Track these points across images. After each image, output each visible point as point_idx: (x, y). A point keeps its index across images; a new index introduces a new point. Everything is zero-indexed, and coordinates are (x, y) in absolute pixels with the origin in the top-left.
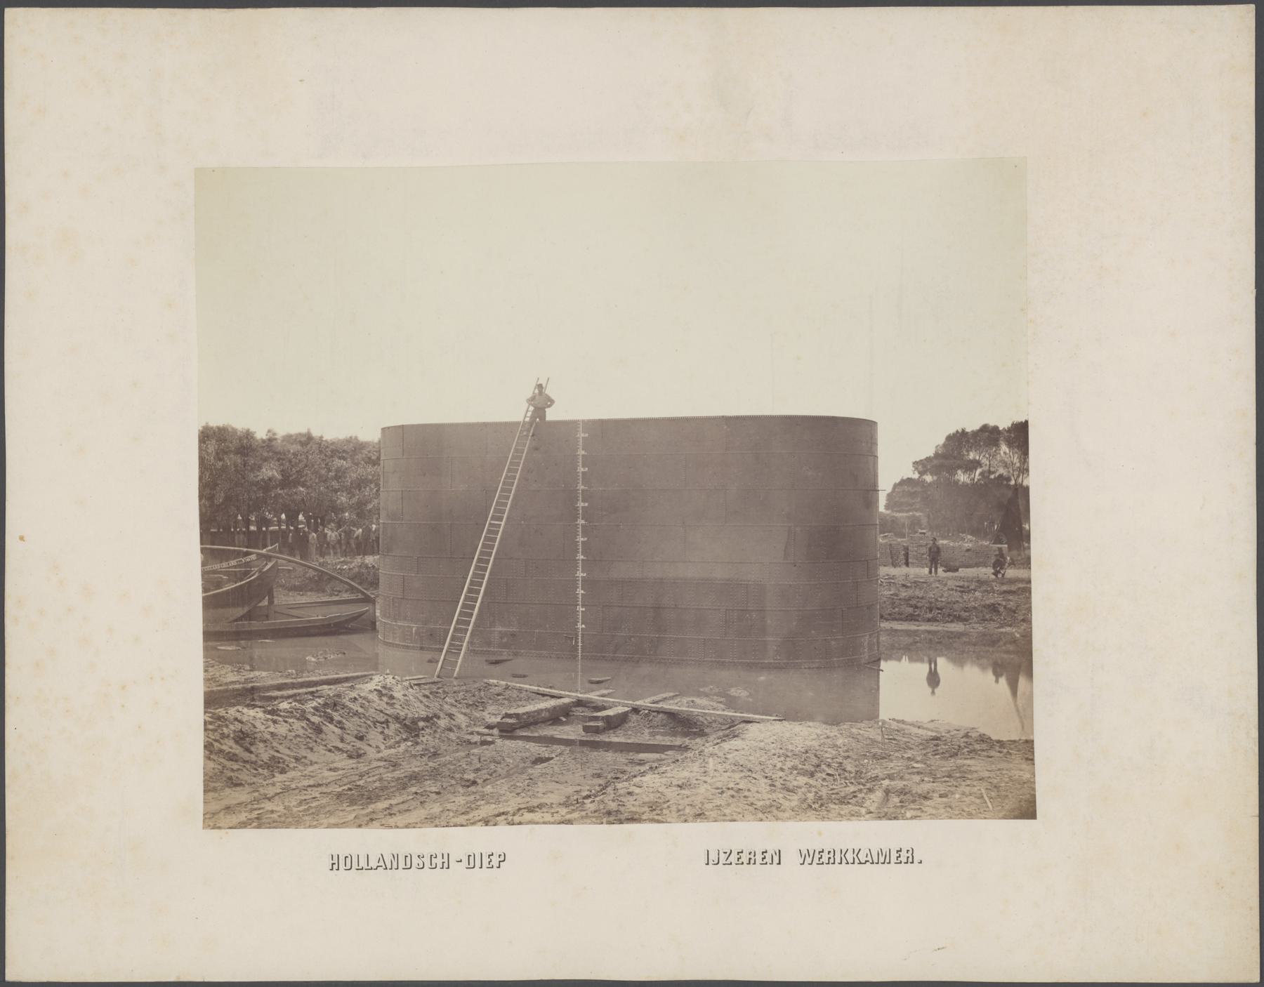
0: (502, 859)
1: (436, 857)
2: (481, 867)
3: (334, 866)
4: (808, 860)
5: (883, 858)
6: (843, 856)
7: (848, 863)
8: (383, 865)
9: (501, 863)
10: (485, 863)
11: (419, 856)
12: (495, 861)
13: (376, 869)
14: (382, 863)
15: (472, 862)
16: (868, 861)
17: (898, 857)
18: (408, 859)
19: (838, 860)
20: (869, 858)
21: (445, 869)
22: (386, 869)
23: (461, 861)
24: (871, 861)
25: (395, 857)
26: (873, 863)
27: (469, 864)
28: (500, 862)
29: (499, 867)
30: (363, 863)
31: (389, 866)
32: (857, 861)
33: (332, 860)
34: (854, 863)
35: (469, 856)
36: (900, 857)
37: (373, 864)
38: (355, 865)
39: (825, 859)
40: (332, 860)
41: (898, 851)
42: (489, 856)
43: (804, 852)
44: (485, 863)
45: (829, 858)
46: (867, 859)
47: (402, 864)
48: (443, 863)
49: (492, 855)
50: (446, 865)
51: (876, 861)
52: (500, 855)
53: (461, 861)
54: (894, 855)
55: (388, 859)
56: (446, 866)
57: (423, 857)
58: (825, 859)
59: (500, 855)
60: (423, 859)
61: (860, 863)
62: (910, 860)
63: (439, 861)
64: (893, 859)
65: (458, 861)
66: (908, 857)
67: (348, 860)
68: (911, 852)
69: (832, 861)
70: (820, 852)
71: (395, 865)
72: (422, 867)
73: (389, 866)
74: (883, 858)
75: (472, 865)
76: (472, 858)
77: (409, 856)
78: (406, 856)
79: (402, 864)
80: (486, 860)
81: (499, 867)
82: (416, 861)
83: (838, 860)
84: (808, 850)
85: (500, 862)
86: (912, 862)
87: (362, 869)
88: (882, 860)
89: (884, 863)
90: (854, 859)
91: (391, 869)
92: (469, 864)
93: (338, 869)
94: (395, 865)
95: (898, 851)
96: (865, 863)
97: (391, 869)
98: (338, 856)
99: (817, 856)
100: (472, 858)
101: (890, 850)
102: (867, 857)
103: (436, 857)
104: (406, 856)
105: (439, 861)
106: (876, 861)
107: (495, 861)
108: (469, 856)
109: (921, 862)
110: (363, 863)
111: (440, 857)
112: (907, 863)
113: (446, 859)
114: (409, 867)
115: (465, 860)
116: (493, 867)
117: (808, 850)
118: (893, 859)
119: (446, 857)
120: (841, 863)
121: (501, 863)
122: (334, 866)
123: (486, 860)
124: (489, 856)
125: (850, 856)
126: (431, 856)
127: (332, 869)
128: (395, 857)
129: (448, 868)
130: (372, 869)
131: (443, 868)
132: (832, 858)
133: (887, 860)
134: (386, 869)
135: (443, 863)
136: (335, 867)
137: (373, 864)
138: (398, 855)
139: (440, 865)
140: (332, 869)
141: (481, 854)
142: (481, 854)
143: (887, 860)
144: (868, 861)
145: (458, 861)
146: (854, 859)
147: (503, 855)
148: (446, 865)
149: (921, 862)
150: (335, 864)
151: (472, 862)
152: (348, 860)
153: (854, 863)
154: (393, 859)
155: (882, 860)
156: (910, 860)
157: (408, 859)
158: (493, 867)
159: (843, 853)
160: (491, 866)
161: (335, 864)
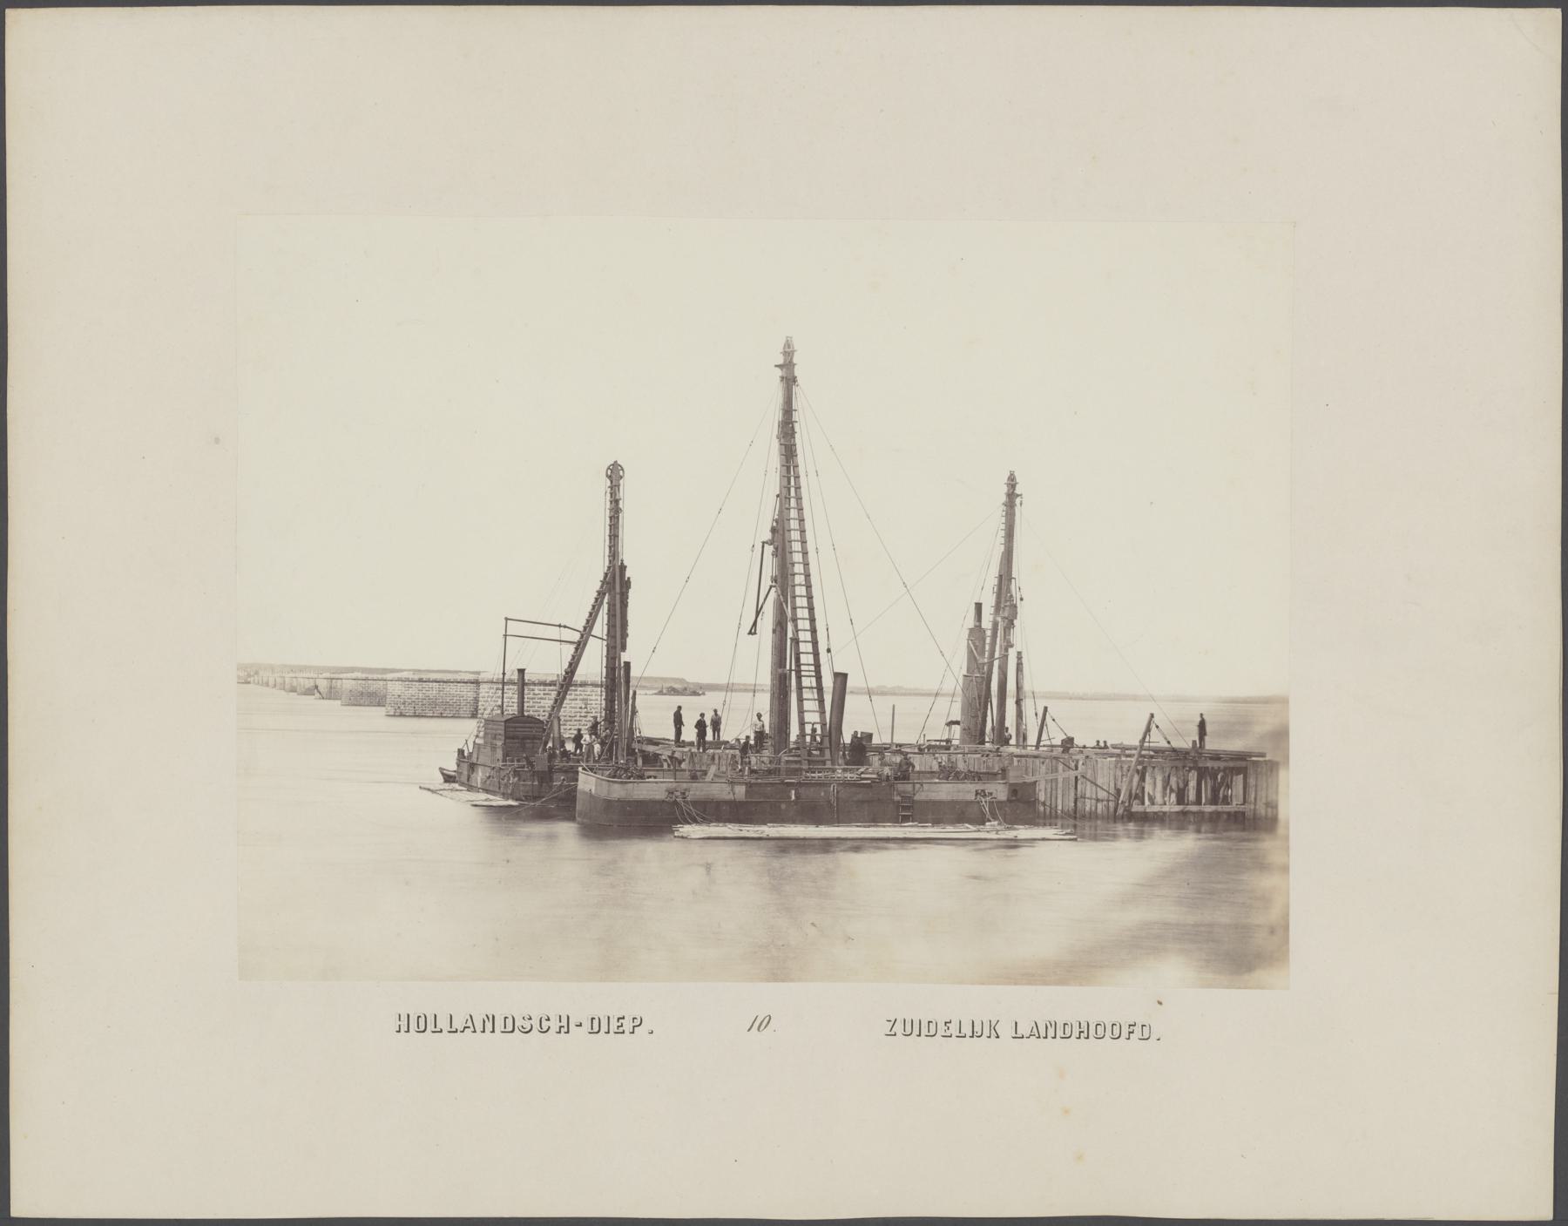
2: (608, 1032)
8: (470, 1025)
12: (628, 1025)
13: (463, 1032)
14: (470, 1024)
15: (596, 1026)
22: (475, 1032)
23: (581, 1025)
27: (592, 1029)
28: (634, 1027)
29: (633, 1033)
30: (443, 1023)
35: (593, 1019)
37: (458, 1024)
38: (430, 1027)
44: (613, 1027)
49: (623, 1018)
53: (581, 1025)
57: (530, 1019)
65: (577, 1026)
85: (634, 1027)
100: (596, 1023)
107: (628, 1025)
108: (593, 1019)
114: (511, 1029)
115: (587, 1025)
130: (456, 1031)
134: (475, 1032)
137: (458, 1024)
138: (493, 1017)
151: (596, 1026)
154: (486, 1020)
160: (621, 1030)
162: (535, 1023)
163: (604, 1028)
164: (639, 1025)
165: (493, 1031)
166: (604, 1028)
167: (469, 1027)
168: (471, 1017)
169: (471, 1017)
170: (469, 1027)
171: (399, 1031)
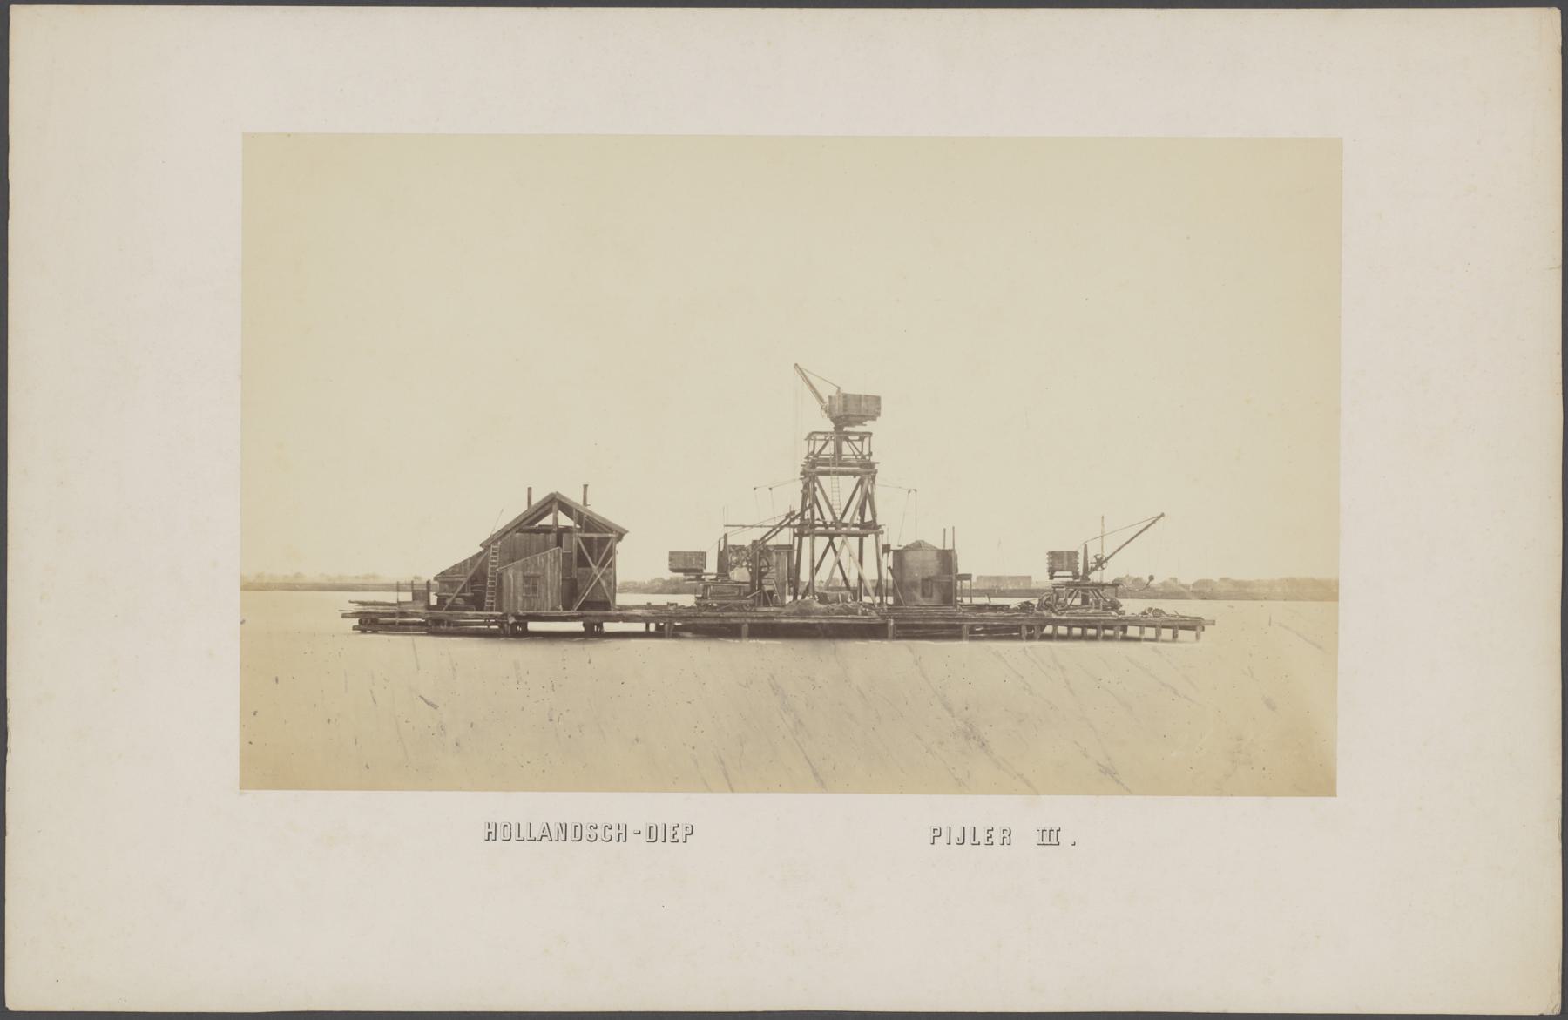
2: (665, 841)
3: (490, 836)
9: (688, 837)
10: (669, 837)
12: (680, 836)
14: (547, 834)
15: (653, 835)
17: (991, 837)
18: (578, 829)
22: (551, 840)
23: (640, 833)
28: (686, 835)
30: (524, 834)
31: (554, 837)
35: (651, 827)
37: (536, 833)
42: (674, 827)
44: (669, 837)
49: (678, 827)
50: (622, 837)
53: (640, 833)
56: (622, 837)
60: (596, 831)
71: (562, 837)
73: (554, 837)
81: (686, 842)
85: (686, 835)
94: (562, 837)
100: (653, 830)
104: (576, 826)
105: (614, 833)
107: (681, 836)
108: (651, 827)
110: (524, 834)
111: (615, 828)
119: (623, 828)
121: (688, 837)
122: (490, 836)
124: (674, 827)
128: (563, 828)
131: (619, 841)
134: (551, 840)
135: (619, 834)
136: (492, 837)
139: (615, 837)
147: (690, 829)
151: (653, 835)
157: (578, 829)
158: (678, 841)
162: (600, 832)
163: (661, 837)
164: (691, 834)
166: (661, 837)
171: (488, 840)
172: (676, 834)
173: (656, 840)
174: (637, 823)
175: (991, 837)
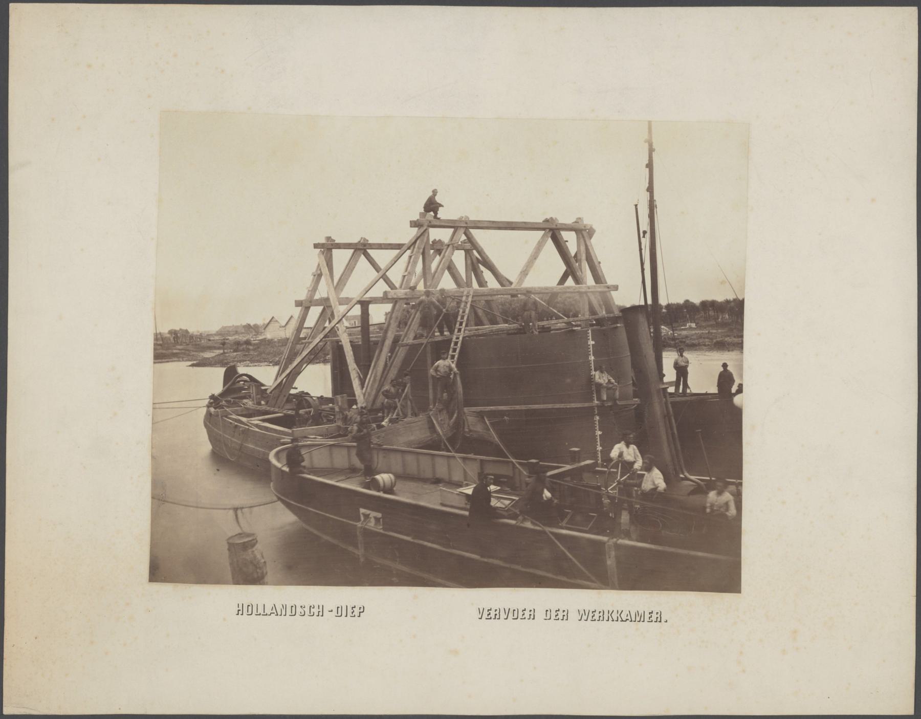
0: (362, 610)
1: (314, 608)
2: (346, 616)
4: (585, 617)
5: (639, 618)
6: (609, 615)
7: (613, 621)
8: (275, 612)
11: (301, 607)
12: (357, 611)
13: (270, 615)
14: (275, 611)
15: (340, 612)
16: (628, 619)
18: (294, 608)
19: (606, 618)
20: (629, 618)
21: (320, 616)
22: (277, 615)
24: (630, 620)
25: (284, 607)
26: (631, 621)
27: (338, 613)
28: (360, 612)
29: (359, 616)
30: (261, 611)
31: (279, 613)
32: (620, 619)
33: (238, 607)
34: (617, 621)
35: (338, 607)
36: (651, 617)
37: (268, 611)
39: (596, 617)
40: (238, 607)
41: (650, 613)
43: (582, 612)
45: (600, 616)
46: (627, 618)
47: (289, 612)
48: (319, 612)
49: (355, 607)
50: (321, 614)
51: (633, 619)
52: (360, 608)
53: (332, 611)
54: (647, 615)
55: (279, 608)
56: (321, 614)
57: (304, 607)
58: (596, 617)
59: (360, 608)
61: (622, 621)
62: (659, 620)
63: (315, 610)
64: (647, 619)
65: (330, 611)
66: (657, 618)
67: (250, 608)
68: (659, 614)
69: (601, 618)
70: (593, 612)
71: (284, 613)
72: (303, 614)
74: (639, 618)
75: (340, 614)
76: (340, 609)
77: (294, 606)
78: (292, 607)
79: (289, 612)
80: (350, 610)
81: (359, 616)
82: (299, 610)
83: (606, 618)
84: (584, 610)
85: (360, 612)
86: (660, 621)
87: (260, 614)
88: (638, 619)
89: (639, 621)
90: (618, 617)
91: (281, 615)
92: (338, 613)
93: (242, 614)
94: (284, 613)
95: (650, 613)
96: (626, 621)
97: (281, 615)
98: (243, 604)
99: (591, 615)
100: (340, 609)
101: (644, 612)
102: (627, 616)
103: (314, 608)
104: (292, 607)
105: (315, 610)
106: (633, 619)
107: (357, 611)
108: (338, 607)
109: (666, 621)
110: (261, 611)
111: (316, 607)
112: (656, 622)
113: (321, 610)
114: (294, 614)
115: (335, 610)
116: (355, 616)
117: (584, 610)
118: (647, 619)
119: (321, 607)
120: (608, 620)
123: (350, 610)
124: (352, 608)
125: (615, 616)
126: (310, 606)
127: (238, 614)
128: (284, 607)
129: (322, 616)
130: (267, 615)
131: (318, 616)
132: (602, 616)
133: (642, 619)
134: (277, 615)
135: (319, 612)
137: (268, 611)
139: (316, 614)
140: (238, 614)
141: (347, 606)
142: (347, 606)
143: (642, 619)
144: (628, 619)
145: (330, 611)
146: (618, 617)
148: (321, 614)
149: (666, 621)
150: (240, 610)
151: (340, 612)
152: (250, 608)
153: (617, 621)
155: (638, 619)
156: (659, 620)
157: (294, 608)
158: (355, 616)
159: (610, 613)
160: (353, 615)
161: (240, 610)
162: (307, 610)
163: (344, 613)
164: (363, 612)
165: (346, 616)
166: (344, 613)
167: (274, 613)
168: (274, 605)
169: (274, 605)
170: (274, 613)
172: (354, 612)
173: (341, 616)
174: (330, 605)
175: (556, 615)
